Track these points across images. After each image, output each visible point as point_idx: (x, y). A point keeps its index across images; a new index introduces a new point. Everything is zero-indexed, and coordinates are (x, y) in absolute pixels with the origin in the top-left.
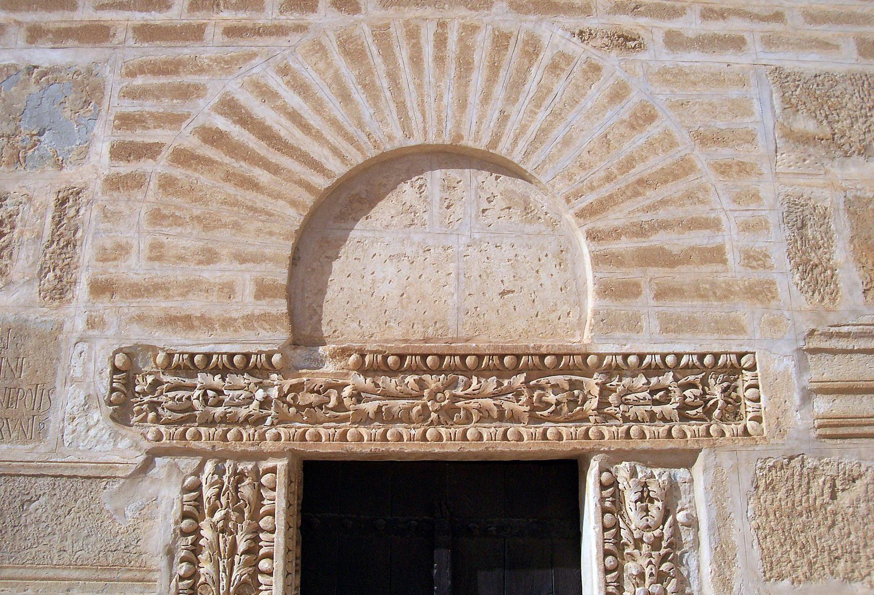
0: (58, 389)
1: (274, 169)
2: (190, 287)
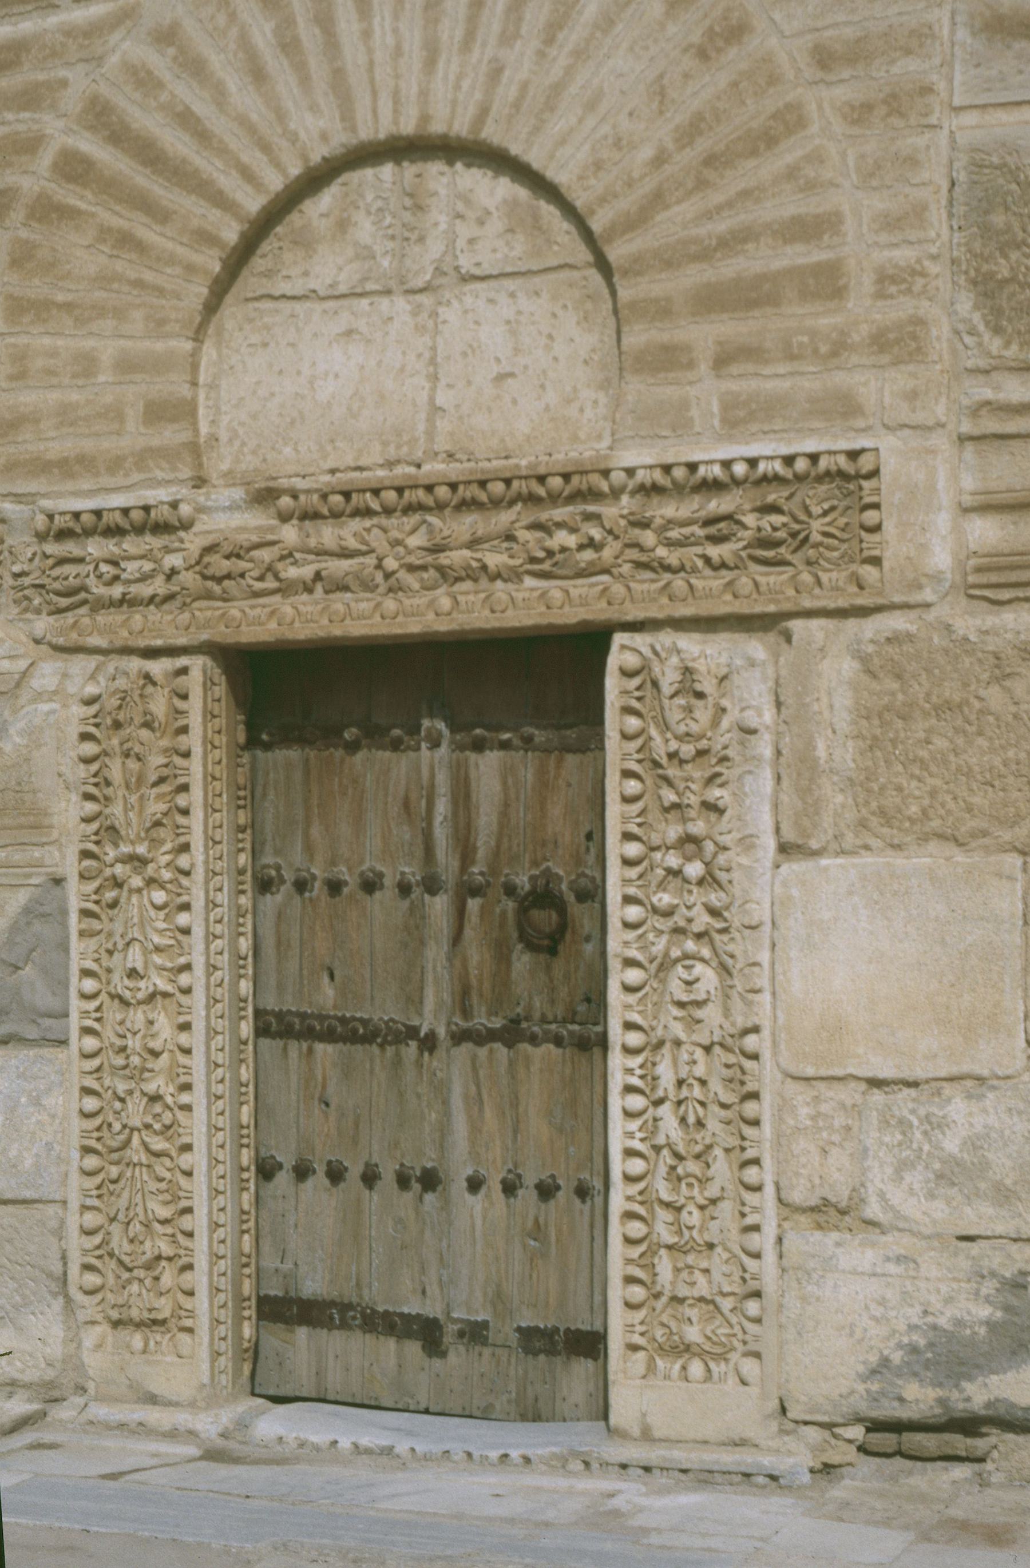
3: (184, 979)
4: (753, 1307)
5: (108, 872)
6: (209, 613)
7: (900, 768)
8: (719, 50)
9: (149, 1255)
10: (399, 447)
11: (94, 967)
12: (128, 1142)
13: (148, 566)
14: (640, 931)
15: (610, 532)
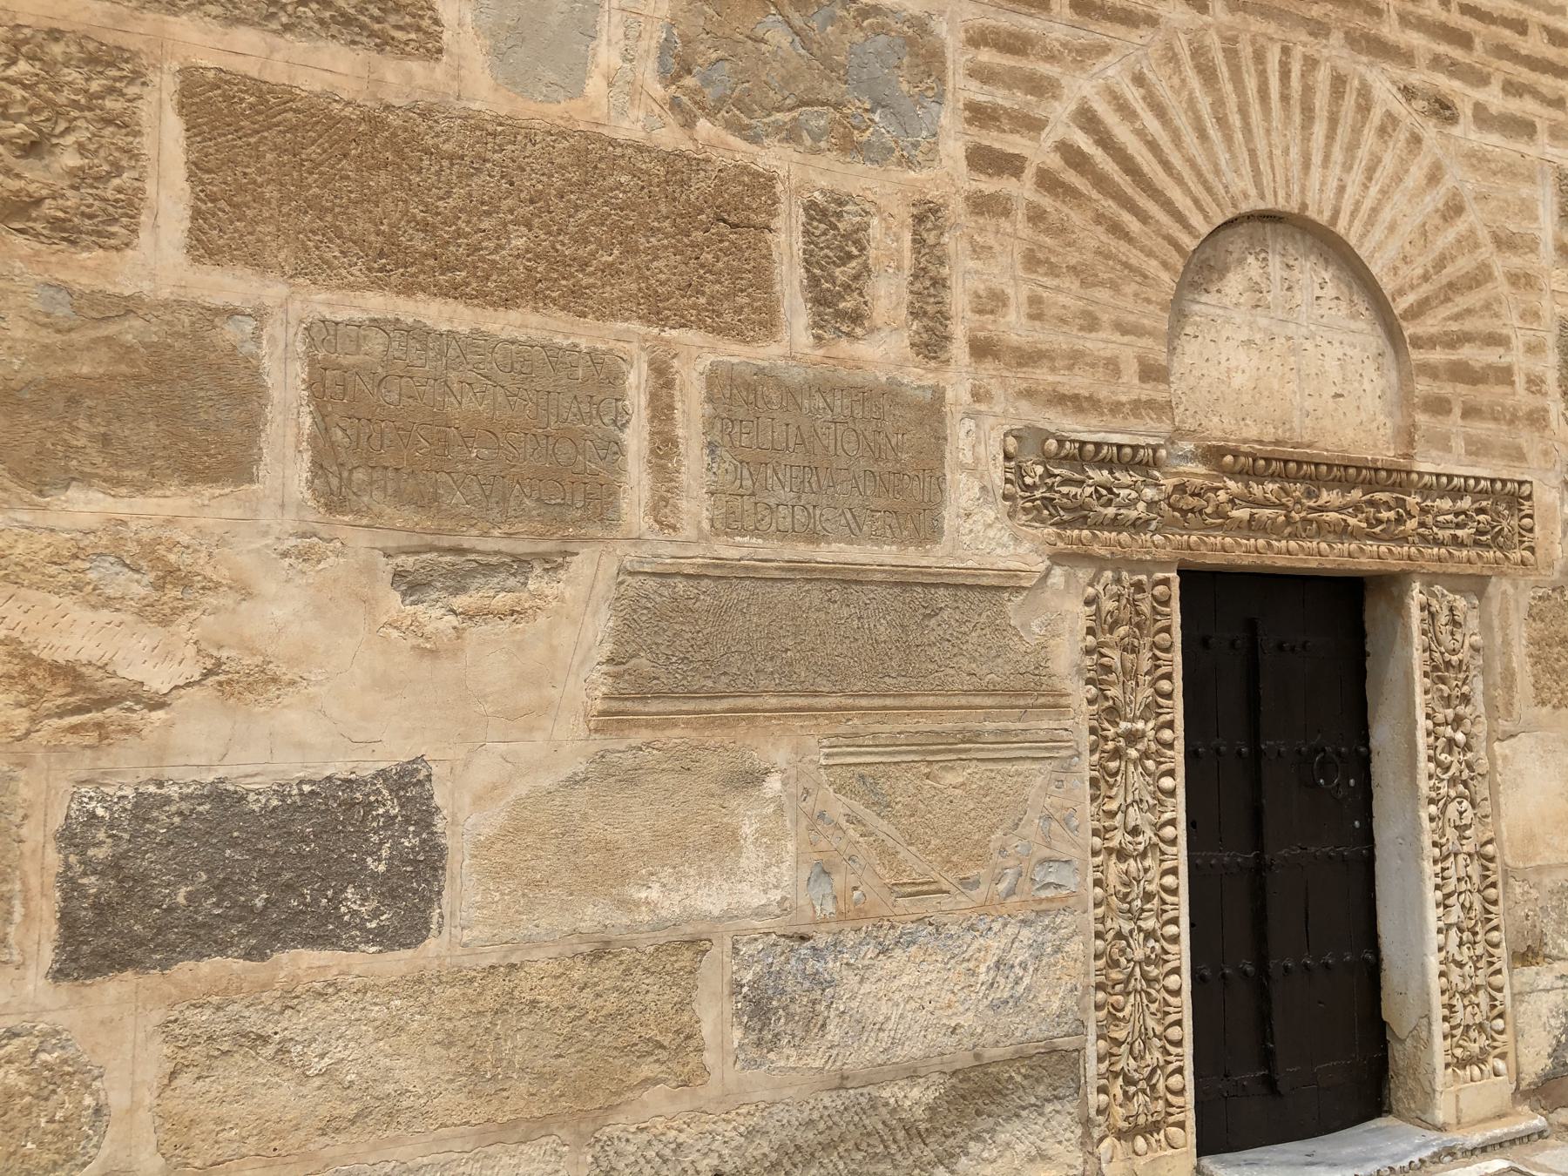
0: (948, 477)
1: (1144, 217)
2: (1075, 358)
4: (1499, 1023)
5: (1110, 745)
12: (1131, 974)
13: (1134, 495)
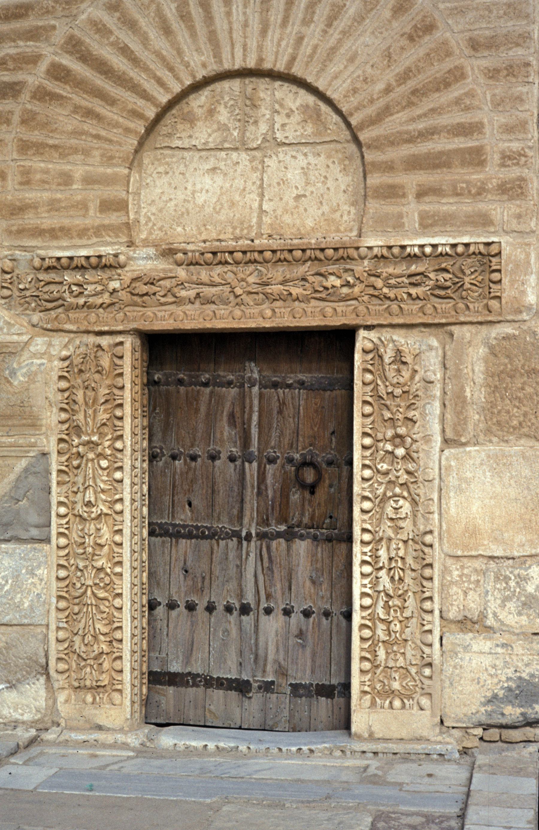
1: (111, 102)
3: (118, 507)
4: (427, 672)
5: (75, 450)
6: (135, 314)
7: (509, 402)
8: (419, 37)
9: (96, 652)
10: (242, 230)
11: (66, 500)
12: (85, 592)
13: (99, 288)
14: (371, 482)
15: (358, 279)
